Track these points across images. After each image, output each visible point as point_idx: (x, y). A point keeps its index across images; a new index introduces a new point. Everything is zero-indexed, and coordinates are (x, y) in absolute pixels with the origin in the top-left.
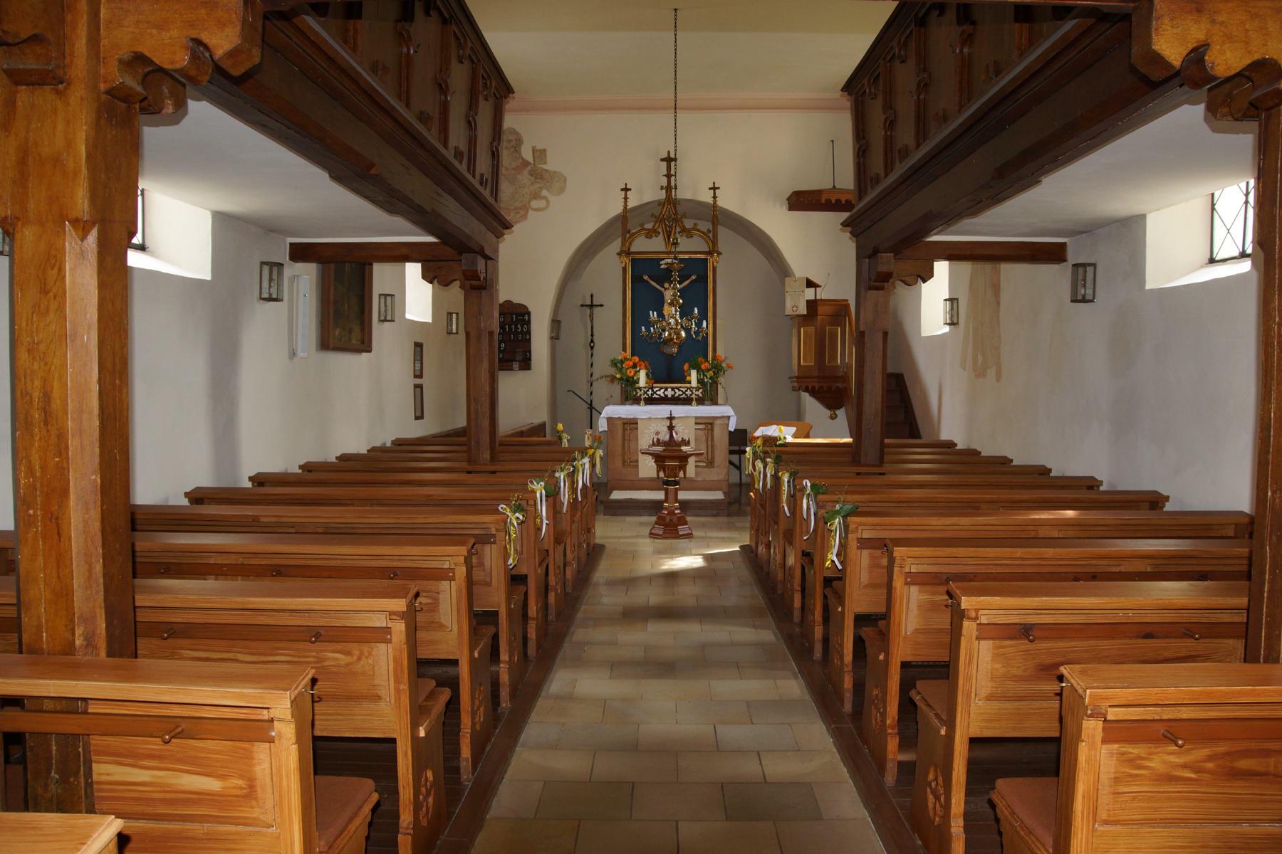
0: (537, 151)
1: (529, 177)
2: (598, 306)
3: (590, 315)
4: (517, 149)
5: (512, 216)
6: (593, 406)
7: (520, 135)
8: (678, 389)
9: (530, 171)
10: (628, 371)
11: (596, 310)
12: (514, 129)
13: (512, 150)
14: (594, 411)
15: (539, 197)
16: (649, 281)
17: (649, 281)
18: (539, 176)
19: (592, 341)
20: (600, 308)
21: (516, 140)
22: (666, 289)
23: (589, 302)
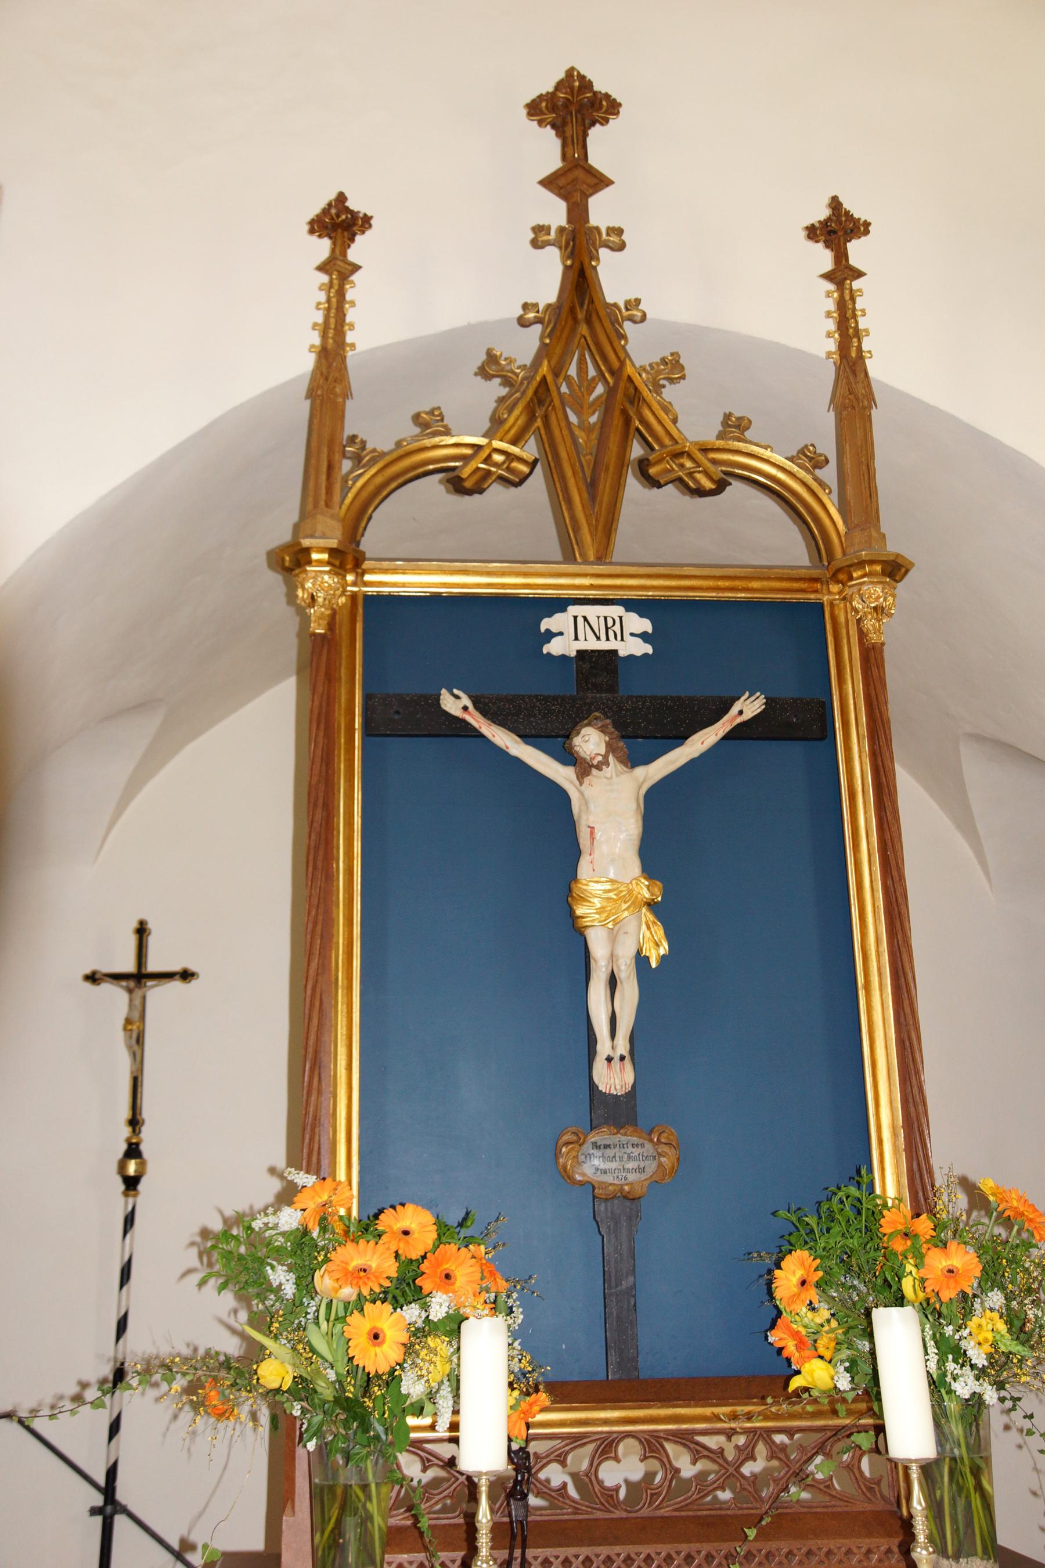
2: (168, 976)
3: (128, 1021)
6: (121, 1496)
8: (684, 1439)
10: (359, 1325)
11: (157, 995)
14: (121, 1522)
16: (476, 720)
17: (476, 720)
19: (133, 1151)
20: (176, 985)
22: (584, 768)
23: (129, 966)
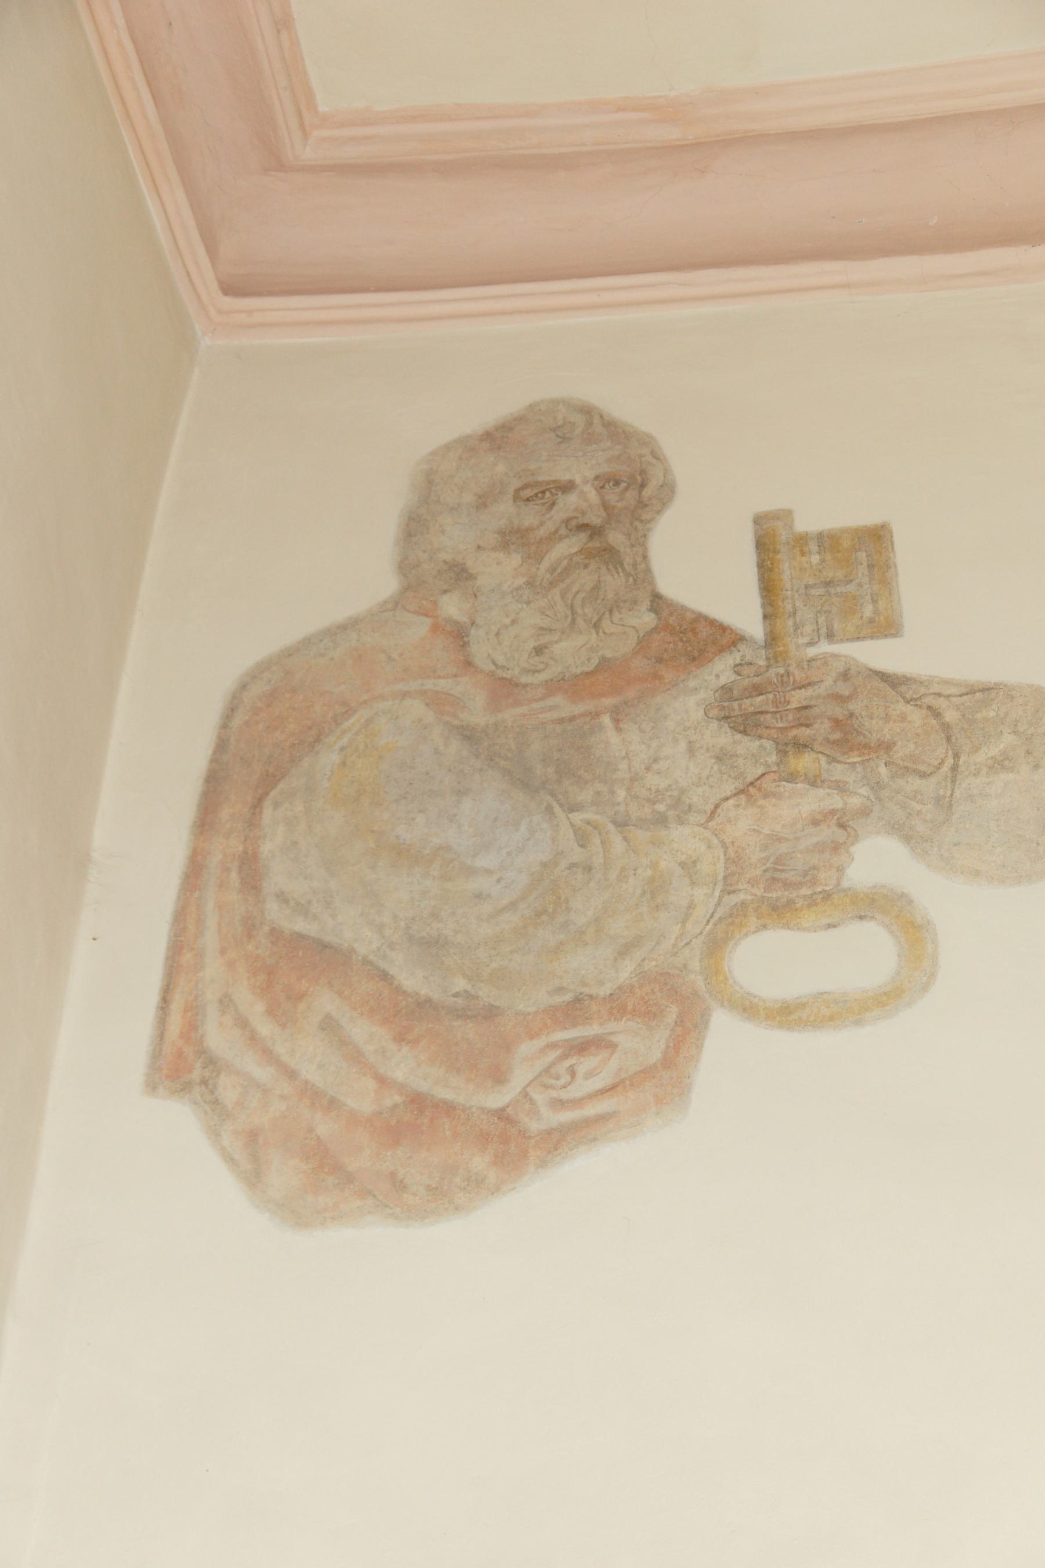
0: (801, 541)
1: (724, 738)
4: (615, 538)
5: (520, 1077)
7: (647, 441)
9: (726, 691)
12: (587, 411)
13: (568, 547)
15: (812, 902)
18: (822, 728)
21: (605, 481)
